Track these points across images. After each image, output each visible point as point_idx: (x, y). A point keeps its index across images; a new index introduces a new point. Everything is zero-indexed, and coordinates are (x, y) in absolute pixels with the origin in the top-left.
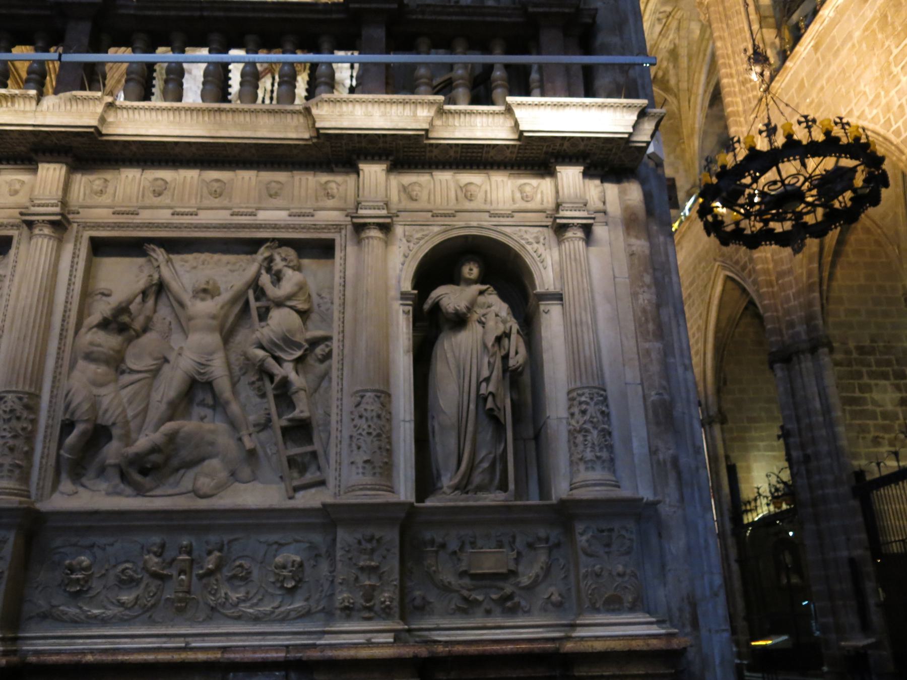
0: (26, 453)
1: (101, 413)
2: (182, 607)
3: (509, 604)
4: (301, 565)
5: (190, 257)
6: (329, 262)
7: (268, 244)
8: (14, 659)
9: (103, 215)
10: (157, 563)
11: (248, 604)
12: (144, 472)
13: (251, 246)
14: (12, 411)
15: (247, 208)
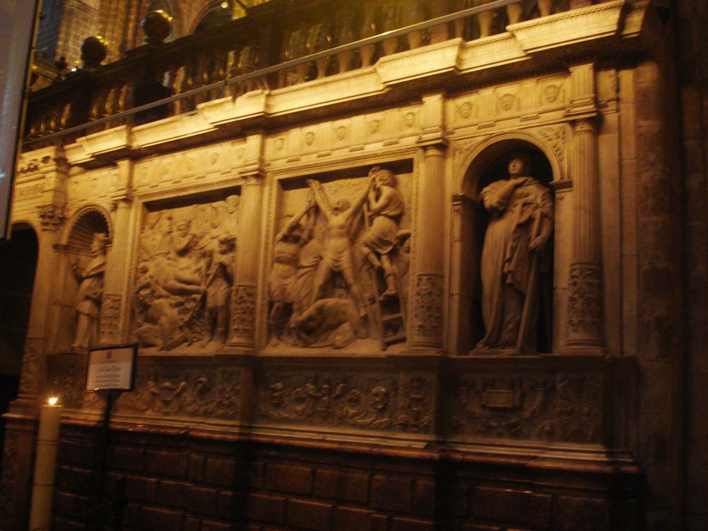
0: (251, 322)
1: (286, 295)
2: (327, 417)
3: (513, 430)
4: (386, 394)
5: (331, 184)
6: (410, 174)
7: (373, 169)
8: (244, 438)
9: (281, 164)
10: (312, 389)
11: (358, 417)
12: (309, 332)
13: (362, 172)
14: (241, 298)
15: (358, 144)
